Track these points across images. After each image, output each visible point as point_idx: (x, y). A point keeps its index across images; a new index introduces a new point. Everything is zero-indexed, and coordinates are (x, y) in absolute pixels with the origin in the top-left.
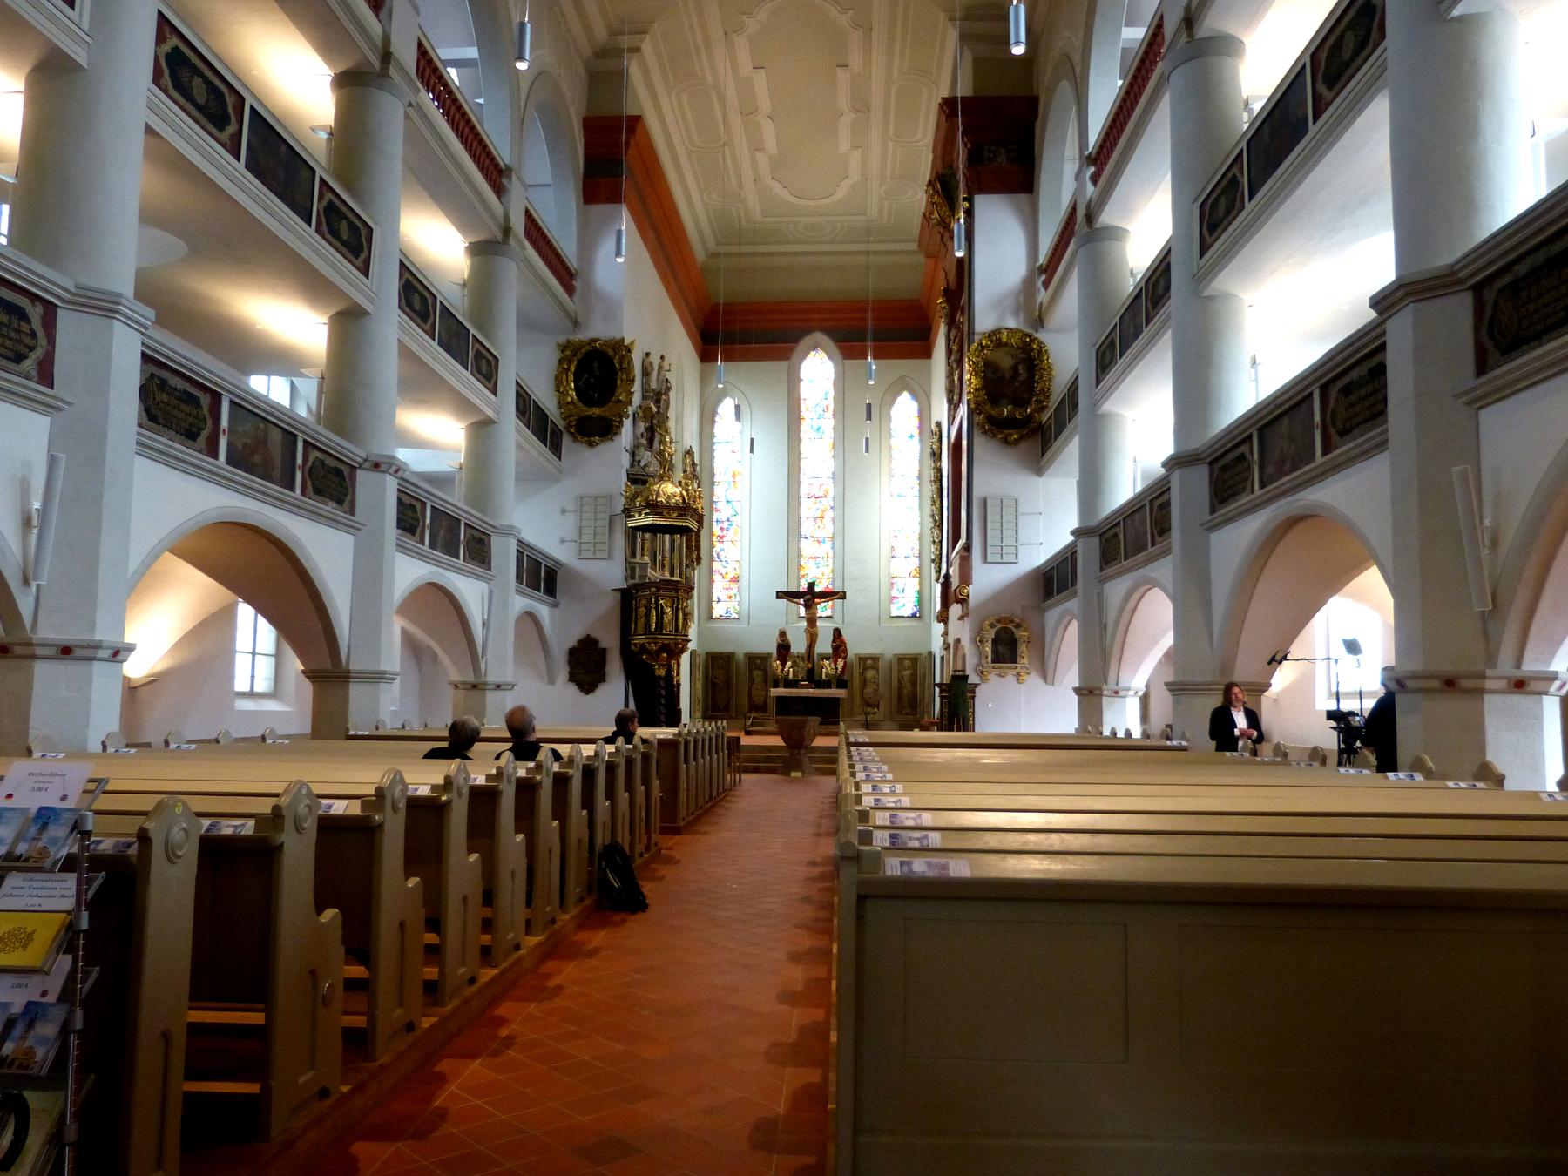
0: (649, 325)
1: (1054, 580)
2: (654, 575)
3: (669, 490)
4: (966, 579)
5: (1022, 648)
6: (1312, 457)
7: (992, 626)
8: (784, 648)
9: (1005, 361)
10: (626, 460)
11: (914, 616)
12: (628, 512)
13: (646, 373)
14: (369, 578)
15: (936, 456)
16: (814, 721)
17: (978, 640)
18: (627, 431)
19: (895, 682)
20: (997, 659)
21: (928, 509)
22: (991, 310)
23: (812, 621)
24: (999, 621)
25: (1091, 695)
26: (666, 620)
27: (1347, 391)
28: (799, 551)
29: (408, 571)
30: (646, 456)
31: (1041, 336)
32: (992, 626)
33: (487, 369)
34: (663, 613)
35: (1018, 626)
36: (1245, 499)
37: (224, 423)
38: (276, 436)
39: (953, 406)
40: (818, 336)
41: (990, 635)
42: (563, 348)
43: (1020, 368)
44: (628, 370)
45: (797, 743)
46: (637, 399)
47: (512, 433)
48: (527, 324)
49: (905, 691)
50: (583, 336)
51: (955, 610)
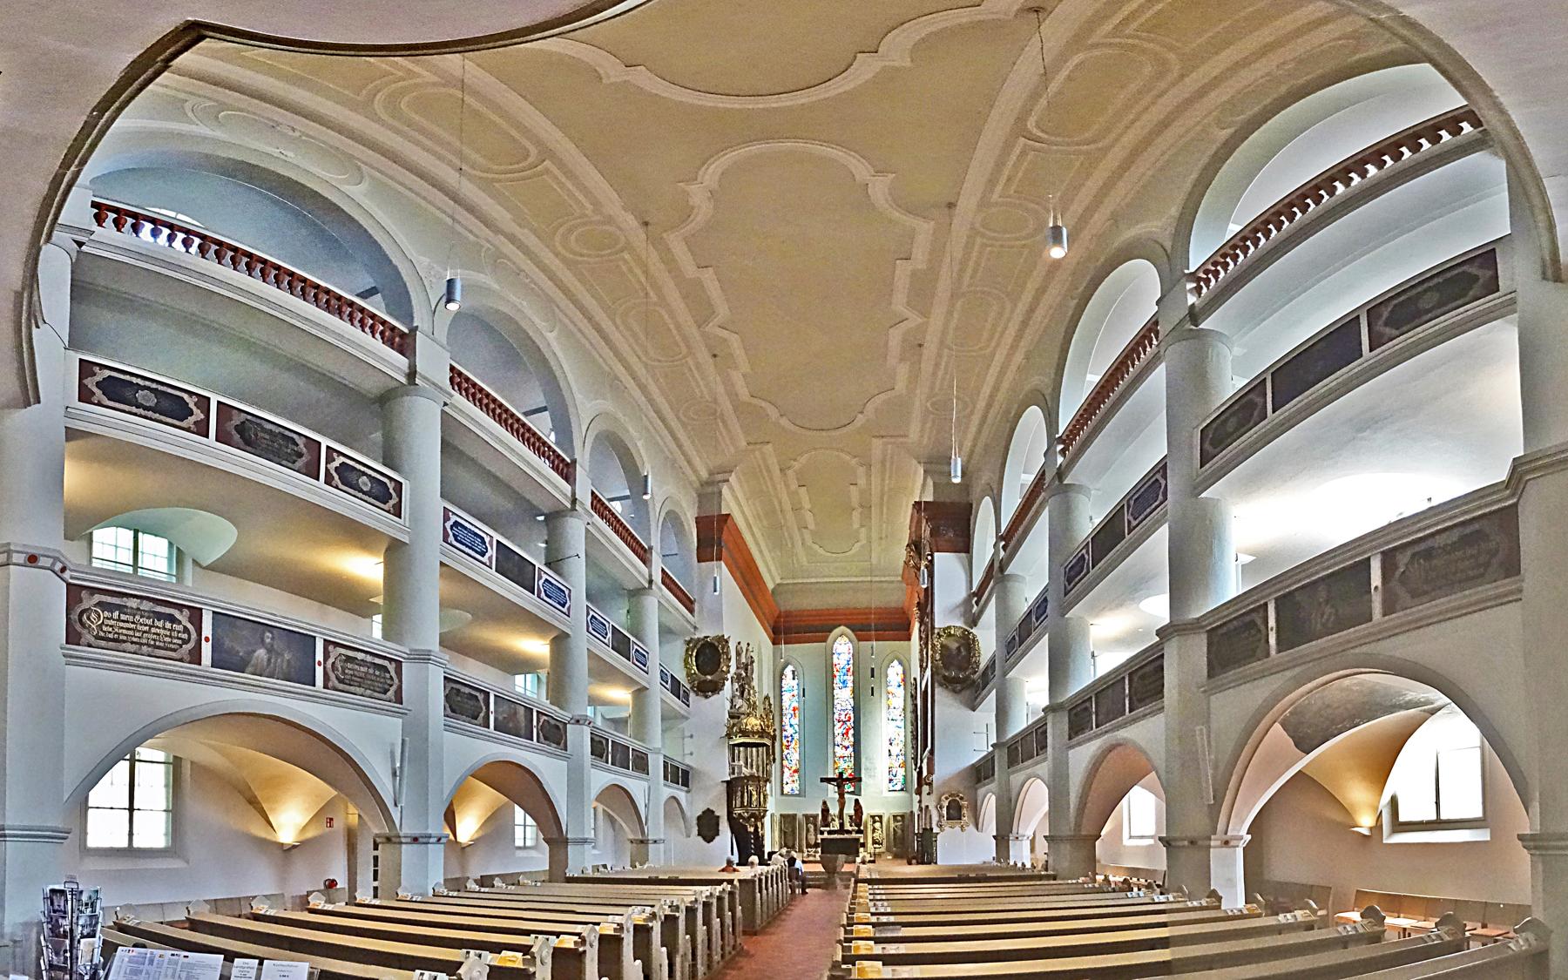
0: (741, 627)
1: (981, 773)
2: (746, 771)
3: (753, 723)
4: (931, 772)
5: (964, 811)
6: (1123, 713)
8: (825, 811)
9: (954, 645)
10: (728, 705)
12: (729, 736)
13: (738, 654)
14: (576, 784)
15: (914, 697)
16: (842, 857)
18: (728, 688)
21: (910, 728)
22: (945, 616)
23: (842, 795)
25: (1002, 840)
27: (1143, 677)
29: (600, 778)
30: (739, 702)
31: (973, 631)
33: (642, 660)
36: (1087, 734)
37: (492, 708)
38: (522, 711)
39: (923, 669)
40: (842, 628)
42: (688, 643)
44: (727, 654)
45: (831, 870)
46: (733, 669)
47: (660, 695)
48: (666, 632)
50: (699, 635)
51: (925, 789)
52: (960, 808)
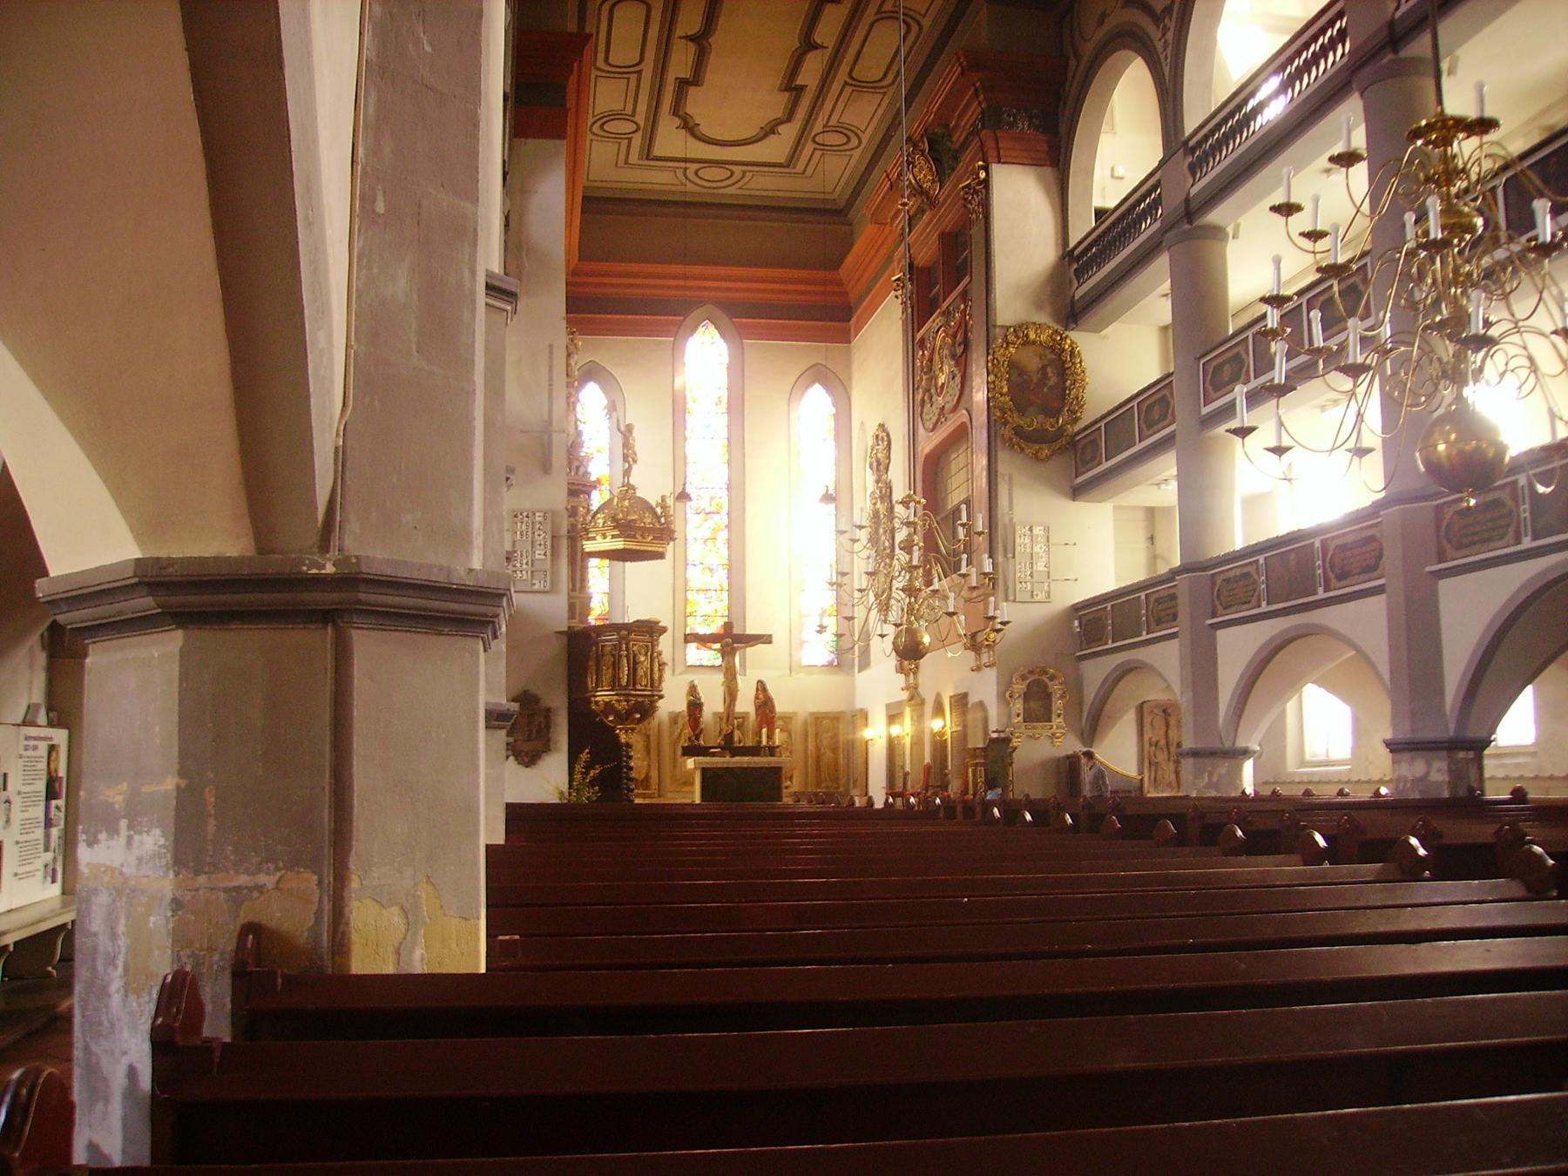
5: (1058, 704)
7: (1023, 678)
8: (695, 706)
11: (830, 664)
17: (1005, 697)
19: (811, 746)
20: (1029, 717)
24: (1031, 672)
26: (640, 672)
28: (686, 581)
32: (1023, 678)
34: (636, 663)
35: (1052, 678)
41: (1020, 687)
43: (1049, 369)
49: (824, 760)
52: (1047, 697)
